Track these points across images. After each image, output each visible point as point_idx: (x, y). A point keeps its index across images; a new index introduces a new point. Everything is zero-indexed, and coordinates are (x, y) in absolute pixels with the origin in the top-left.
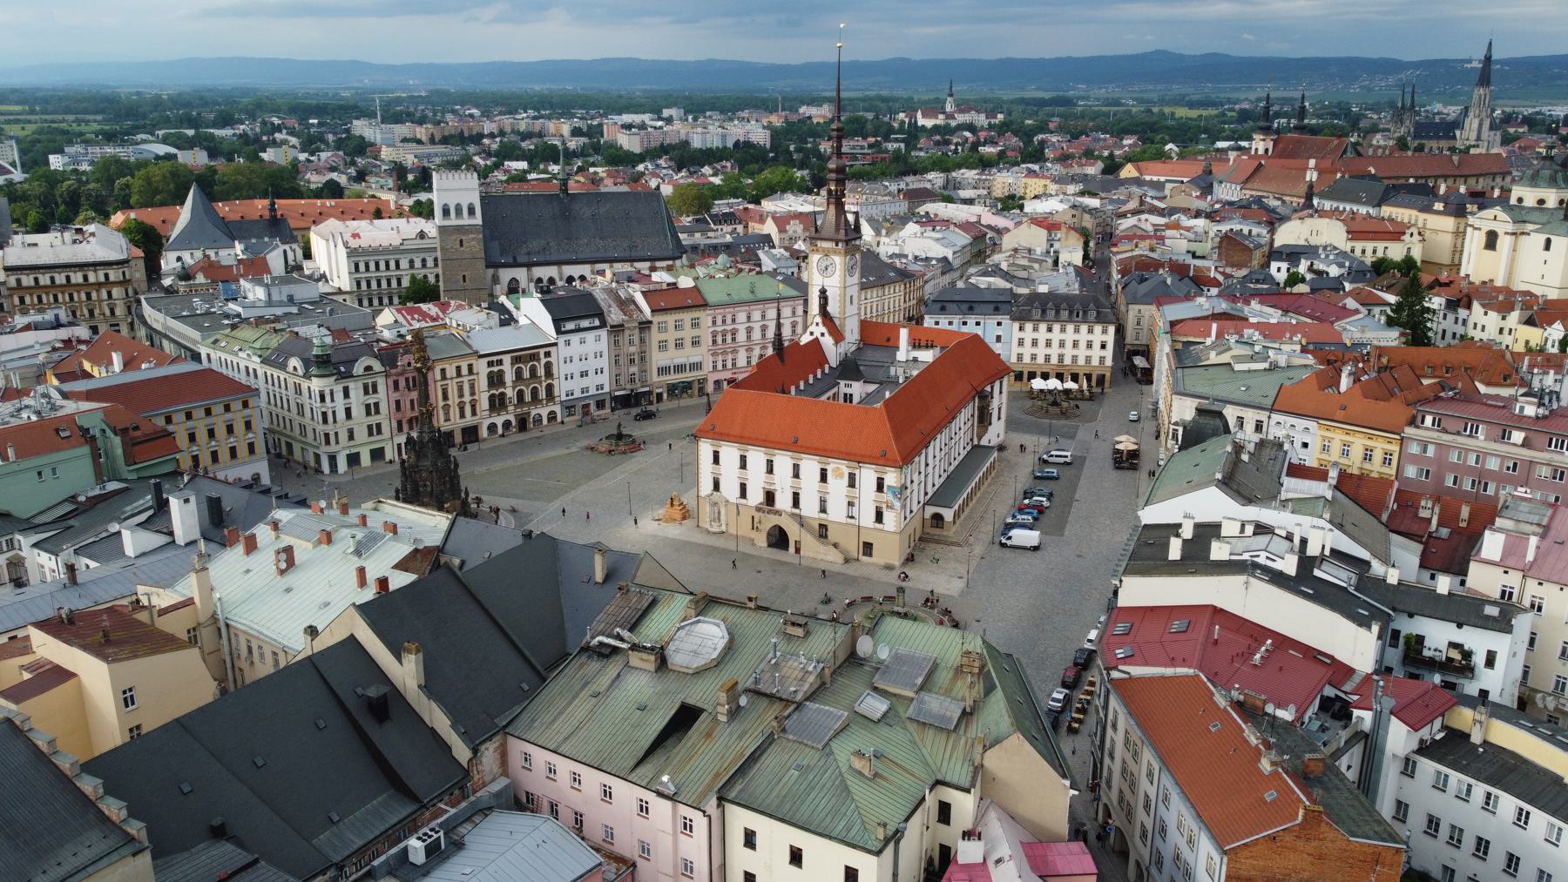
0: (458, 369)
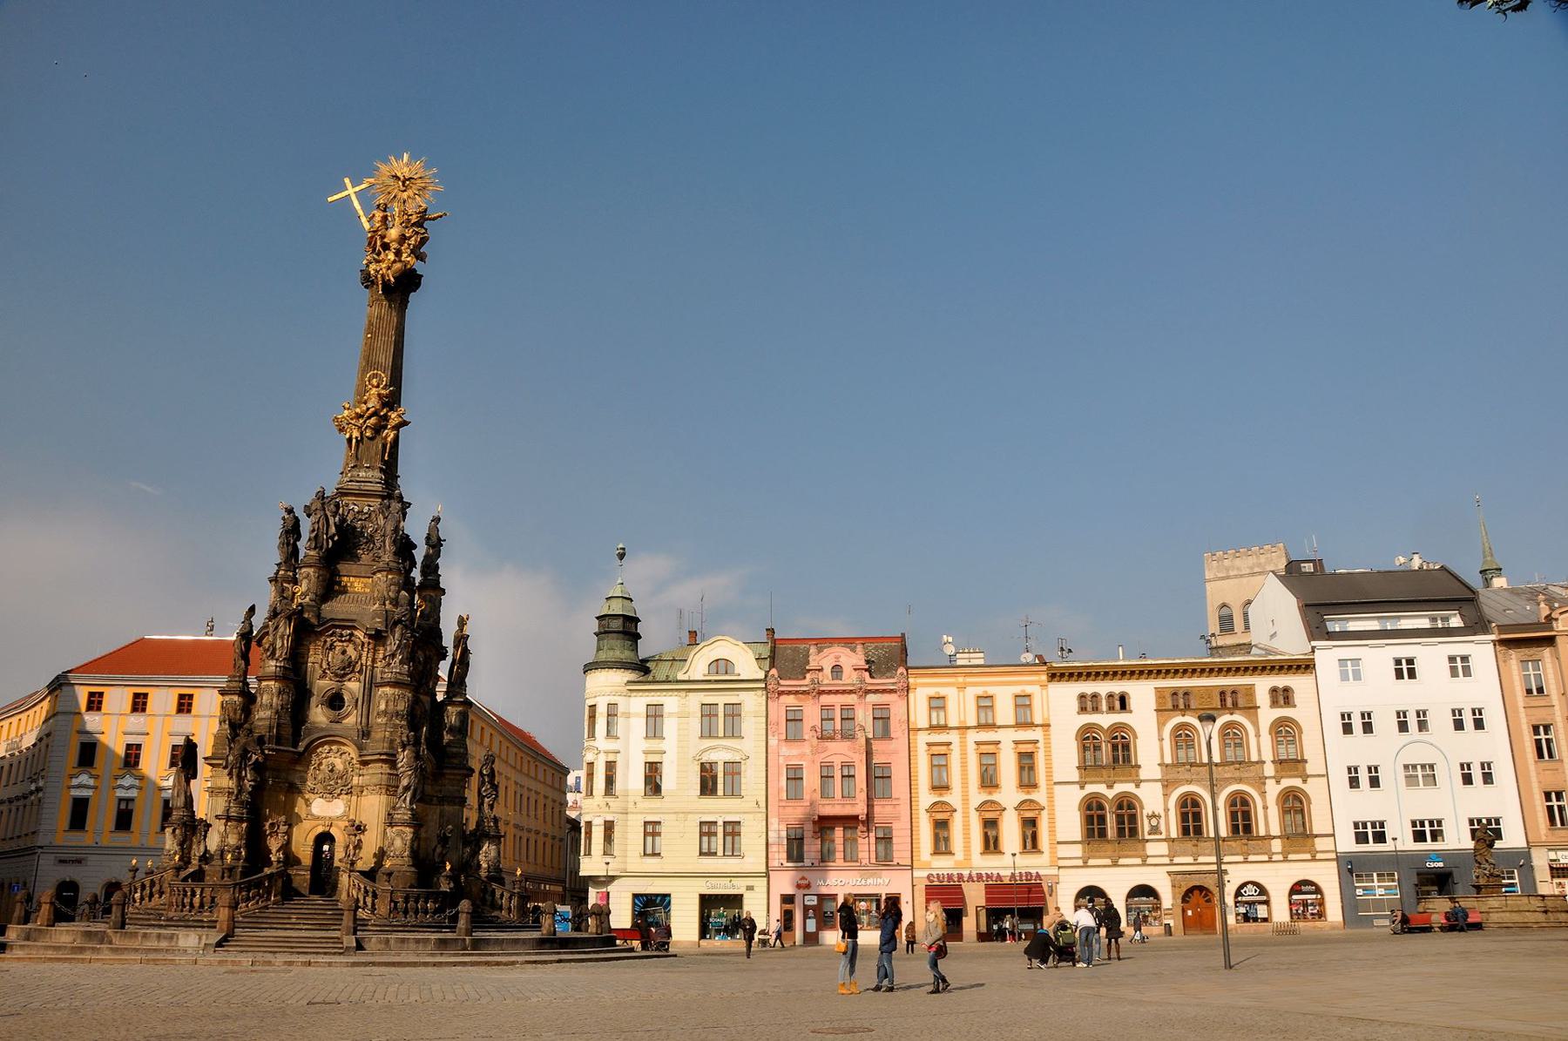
0: (985, 703)
